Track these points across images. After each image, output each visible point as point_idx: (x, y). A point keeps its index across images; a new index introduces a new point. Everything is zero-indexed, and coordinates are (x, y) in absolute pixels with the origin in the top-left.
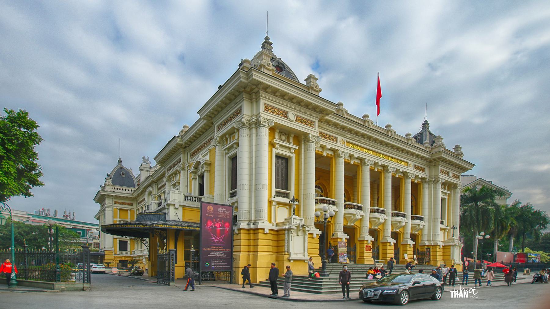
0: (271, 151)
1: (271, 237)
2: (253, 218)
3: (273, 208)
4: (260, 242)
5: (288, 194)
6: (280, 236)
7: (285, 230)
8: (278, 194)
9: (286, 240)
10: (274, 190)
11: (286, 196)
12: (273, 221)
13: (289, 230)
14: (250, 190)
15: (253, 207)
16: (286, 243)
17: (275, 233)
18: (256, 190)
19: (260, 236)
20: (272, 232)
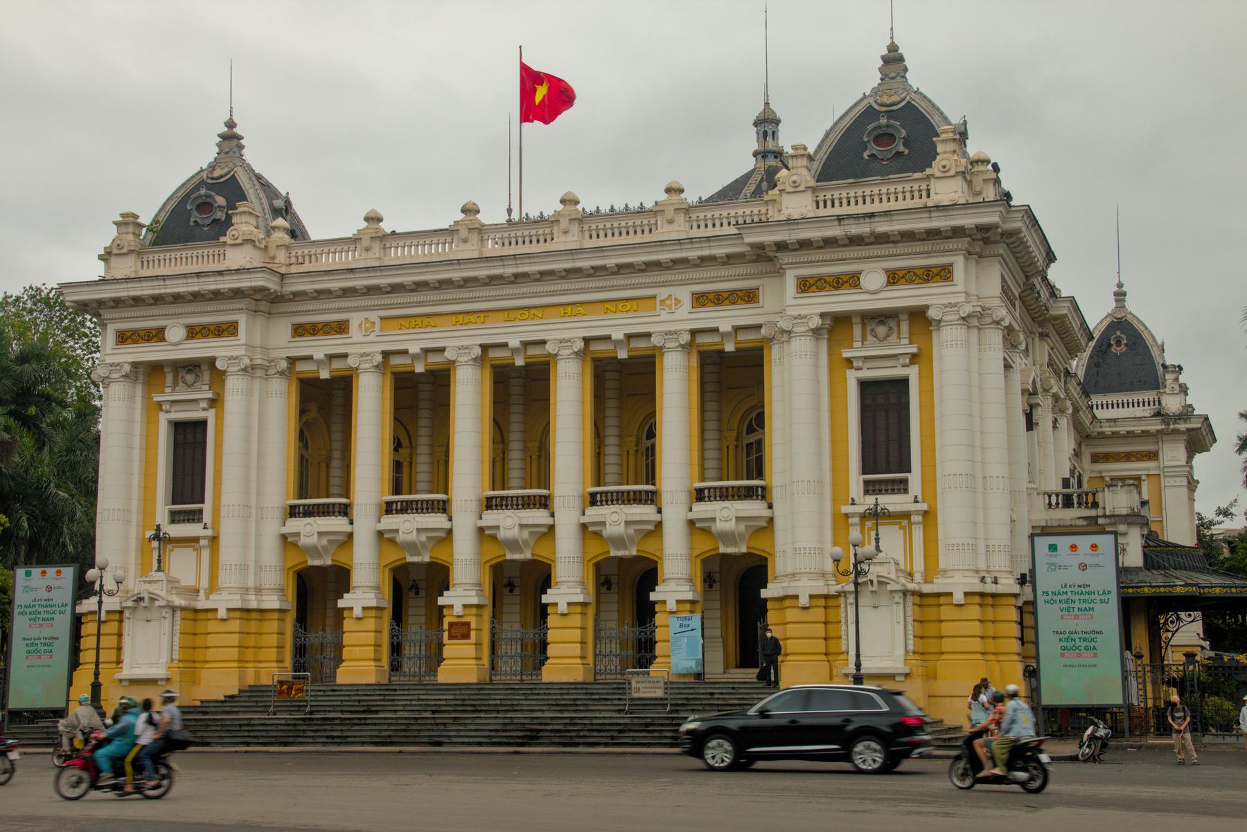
5: (905, 481)
9: (843, 620)
10: (856, 480)
11: (901, 487)
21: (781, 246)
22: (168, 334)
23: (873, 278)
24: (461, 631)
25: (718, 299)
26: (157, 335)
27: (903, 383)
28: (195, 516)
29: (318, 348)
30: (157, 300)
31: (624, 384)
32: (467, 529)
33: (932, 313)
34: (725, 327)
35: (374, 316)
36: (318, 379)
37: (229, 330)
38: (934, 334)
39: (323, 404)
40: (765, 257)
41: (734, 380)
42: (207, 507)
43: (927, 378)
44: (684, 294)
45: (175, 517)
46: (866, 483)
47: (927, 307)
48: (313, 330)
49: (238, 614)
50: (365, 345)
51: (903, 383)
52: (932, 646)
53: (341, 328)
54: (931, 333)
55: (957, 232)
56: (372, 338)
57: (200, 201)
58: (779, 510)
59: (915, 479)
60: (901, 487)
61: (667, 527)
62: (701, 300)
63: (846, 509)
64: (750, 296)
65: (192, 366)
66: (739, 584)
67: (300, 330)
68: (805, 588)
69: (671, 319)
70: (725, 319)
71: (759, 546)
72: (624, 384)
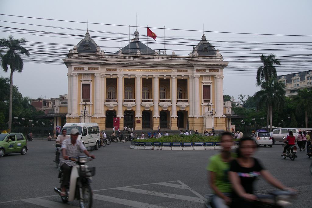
0: (200, 86)
1: (199, 120)
2: (193, 113)
3: (203, 108)
4: (195, 122)
6: (203, 118)
7: (204, 117)
8: (205, 101)
10: (203, 100)
11: (209, 101)
12: (203, 113)
13: (205, 117)
14: (193, 102)
15: (193, 109)
16: (205, 122)
17: (202, 118)
18: (194, 102)
19: (195, 120)
20: (199, 118)
21: (195, 64)
22: (85, 69)
23: (208, 71)
24: (138, 121)
25: (181, 71)
26: (83, 69)
27: (209, 86)
28: (89, 101)
29: (112, 73)
30: (84, 63)
31: (165, 83)
32: (138, 106)
33: (216, 76)
34: (183, 75)
35: (122, 68)
36: (110, 78)
37: (97, 69)
38: (215, 80)
39: (111, 83)
40: (191, 66)
41: (183, 84)
42: (91, 100)
43: (214, 85)
44: (176, 70)
45: (84, 101)
46: (204, 100)
47: (215, 75)
48: (110, 70)
49: (100, 118)
50: (121, 73)
51: (209, 86)
52: (193, 125)
53: (116, 70)
54: (214, 79)
55: (221, 65)
56: (121, 72)
57: (86, 45)
58: (191, 104)
59: (211, 100)
60: (209, 101)
61: (137, 106)
62: (179, 71)
63: (202, 104)
64: (187, 71)
65: (88, 74)
66: (182, 115)
67: (107, 70)
68: (197, 116)
69: (174, 74)
70: (183, 74)
71: (187, 109)
72: (165, 83)
